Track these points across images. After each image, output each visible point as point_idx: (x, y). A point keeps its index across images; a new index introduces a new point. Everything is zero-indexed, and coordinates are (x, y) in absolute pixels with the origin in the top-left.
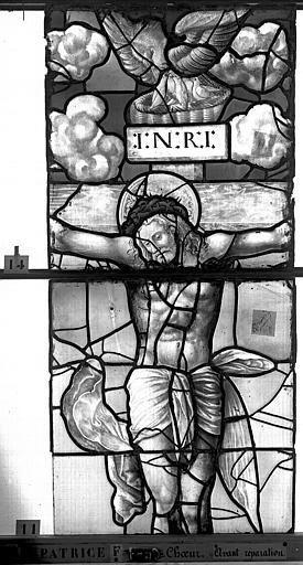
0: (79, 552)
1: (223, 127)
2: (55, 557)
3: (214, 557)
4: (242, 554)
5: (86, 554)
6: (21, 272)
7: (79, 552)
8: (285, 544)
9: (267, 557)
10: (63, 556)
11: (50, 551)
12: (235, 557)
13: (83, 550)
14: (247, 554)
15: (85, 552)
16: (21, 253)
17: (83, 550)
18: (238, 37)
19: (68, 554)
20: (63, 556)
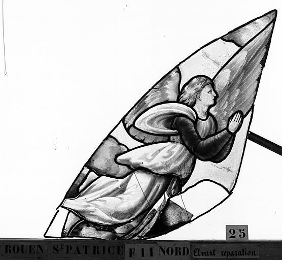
0: (101, 250)
2: (79, 253)
3: (193, 256)
4: (218, 255)
5: (107, 251)
7: (101, 250)
9: (242, 257)
10: (86, 253)
11: (74, 249)
12: (213, 257)
13: (104, 247)
14: (223, 254)
15: (107, 251)
17: (104, 247)
19: (91, 250)
20: (86, 253)
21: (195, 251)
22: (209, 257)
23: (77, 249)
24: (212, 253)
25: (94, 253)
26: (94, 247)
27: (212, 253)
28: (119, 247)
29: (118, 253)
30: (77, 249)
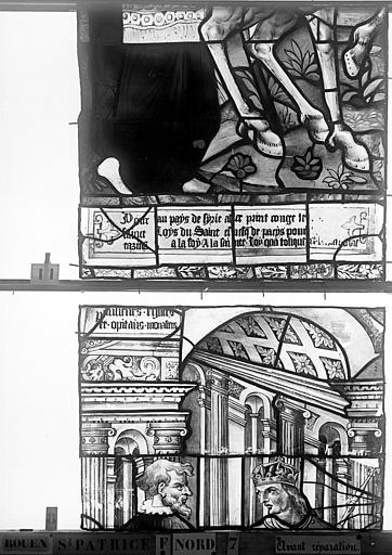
0: (121, 547)
1: (338, 23)
2: (92, 548)
5: (128, 547)
6: (52, 283)
7: (121, 547)
8: (359, 537)
10: (102, 548)
13: (125, 541)
15: (128, 542)
16: (53, 260)
17: (125, 541)
18: (201, 191)
20: (102, 548)
21: (279, 544)
22: (297, 551)
23: (90, 543)
24: (302, 547)
25: (112, 548)
26: (112, 541)
27: (302, 547)
28: (143, 540)
29: (143, 548)
30: (90, 543)
